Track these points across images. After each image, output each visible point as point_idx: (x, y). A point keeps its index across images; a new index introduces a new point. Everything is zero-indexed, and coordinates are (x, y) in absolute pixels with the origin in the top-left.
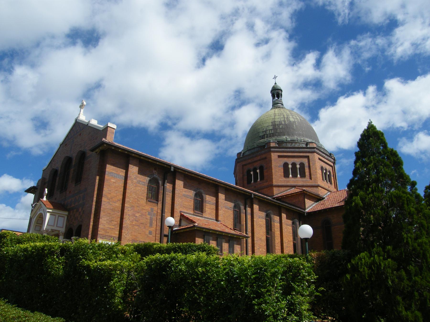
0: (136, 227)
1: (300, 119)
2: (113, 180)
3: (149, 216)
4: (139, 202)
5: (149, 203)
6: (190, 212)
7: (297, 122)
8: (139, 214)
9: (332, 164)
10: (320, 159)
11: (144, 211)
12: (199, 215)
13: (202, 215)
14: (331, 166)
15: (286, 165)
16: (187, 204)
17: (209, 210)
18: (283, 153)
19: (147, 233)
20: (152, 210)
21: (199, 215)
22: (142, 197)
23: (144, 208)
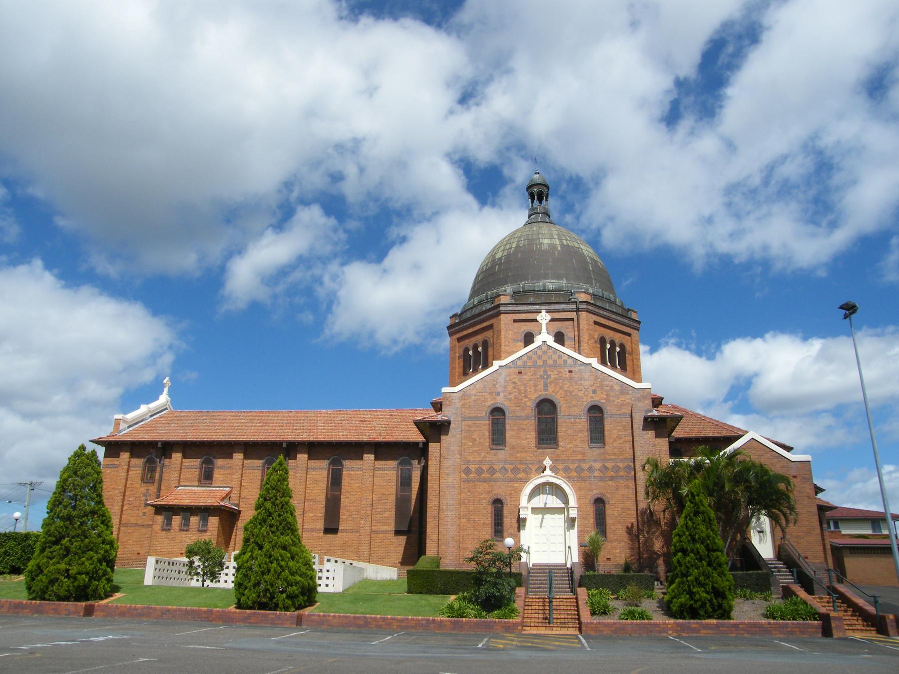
0: (129, 511)
1: (518, 247)
2: (108, 472)
3: (144, 498)
4: (133, 486)
5: (145, 484)
6: (194, 484)
7: (503, 258)
8: (133, 498)
9: (573, 315)
10: (515, 321)
11: (138, 494)
12: (206, 485)
13: (211, 484)
14: (572, 320)
15: (466, 350)
16: (191, 476)
17: (222, 476)
18: (462, 333)
19: (141, 514)
20: (148, 490)
21: (206, 485)
22: (137, 481)
23: (138, 491)
